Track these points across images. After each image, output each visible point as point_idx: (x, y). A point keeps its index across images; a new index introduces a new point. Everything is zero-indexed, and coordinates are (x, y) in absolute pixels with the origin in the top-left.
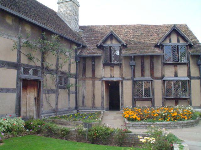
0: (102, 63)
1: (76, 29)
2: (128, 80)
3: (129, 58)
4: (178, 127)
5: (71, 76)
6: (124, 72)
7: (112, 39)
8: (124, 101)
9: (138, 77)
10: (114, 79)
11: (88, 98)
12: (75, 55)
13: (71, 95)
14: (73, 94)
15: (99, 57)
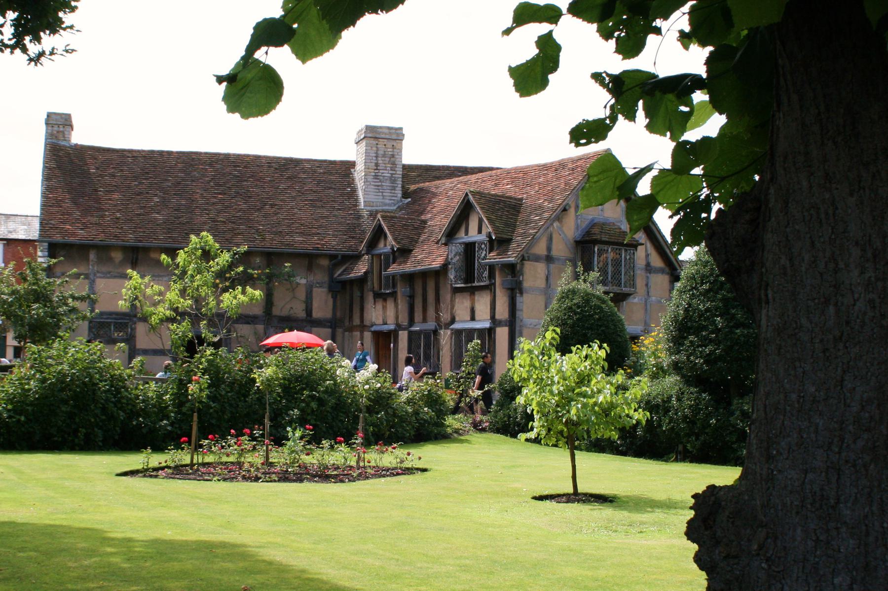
10: (385, 328)
12: (326, 279)
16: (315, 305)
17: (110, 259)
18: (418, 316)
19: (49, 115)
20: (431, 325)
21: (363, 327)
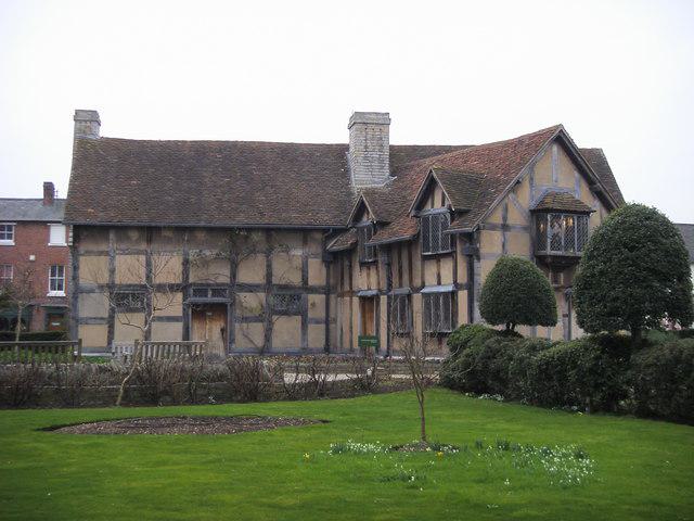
1: (375, 183)
5: (313, 290)
10: (369, 293)
12: (320, 250)
13: (311, 327)
14: (317, 322)
16: (311, 274)
17: (128, 238)
18: (395, 281)
19: (77, 112)
20: (406, 289)
21: (352, 293)
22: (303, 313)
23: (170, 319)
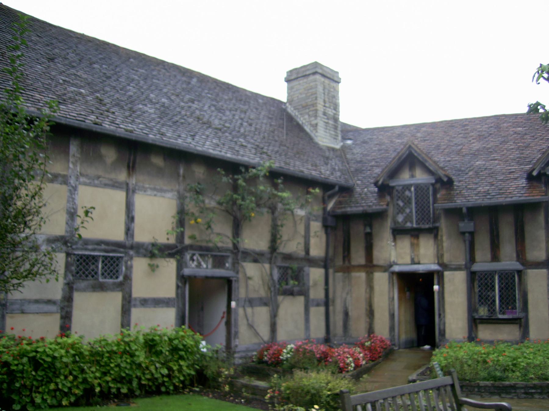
0: (389, 228)
2: (458, 268)
3: (455, 213)
4: (536, 396)
5: (312, 262)
6: (445, 249)
7: (412, 167)
8: (447, 325)
9: (483, 263)
10: (421, 268)
11: (358, 313)
12: (320, 213)
14: (318, 305)
15: (380, 215)
17: (100, 158)
18: (483, 254)
20: (508, 262)
21: (370, 266)
22: (304, 293)
23: (158, 302)
